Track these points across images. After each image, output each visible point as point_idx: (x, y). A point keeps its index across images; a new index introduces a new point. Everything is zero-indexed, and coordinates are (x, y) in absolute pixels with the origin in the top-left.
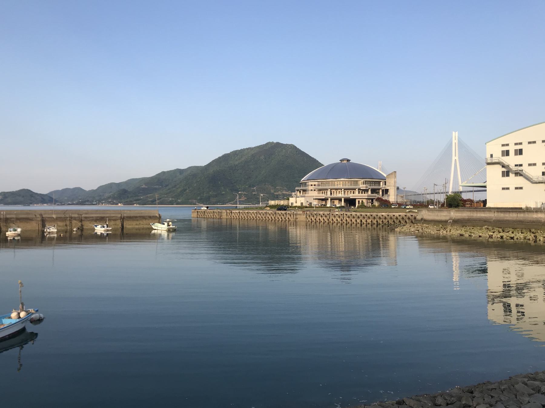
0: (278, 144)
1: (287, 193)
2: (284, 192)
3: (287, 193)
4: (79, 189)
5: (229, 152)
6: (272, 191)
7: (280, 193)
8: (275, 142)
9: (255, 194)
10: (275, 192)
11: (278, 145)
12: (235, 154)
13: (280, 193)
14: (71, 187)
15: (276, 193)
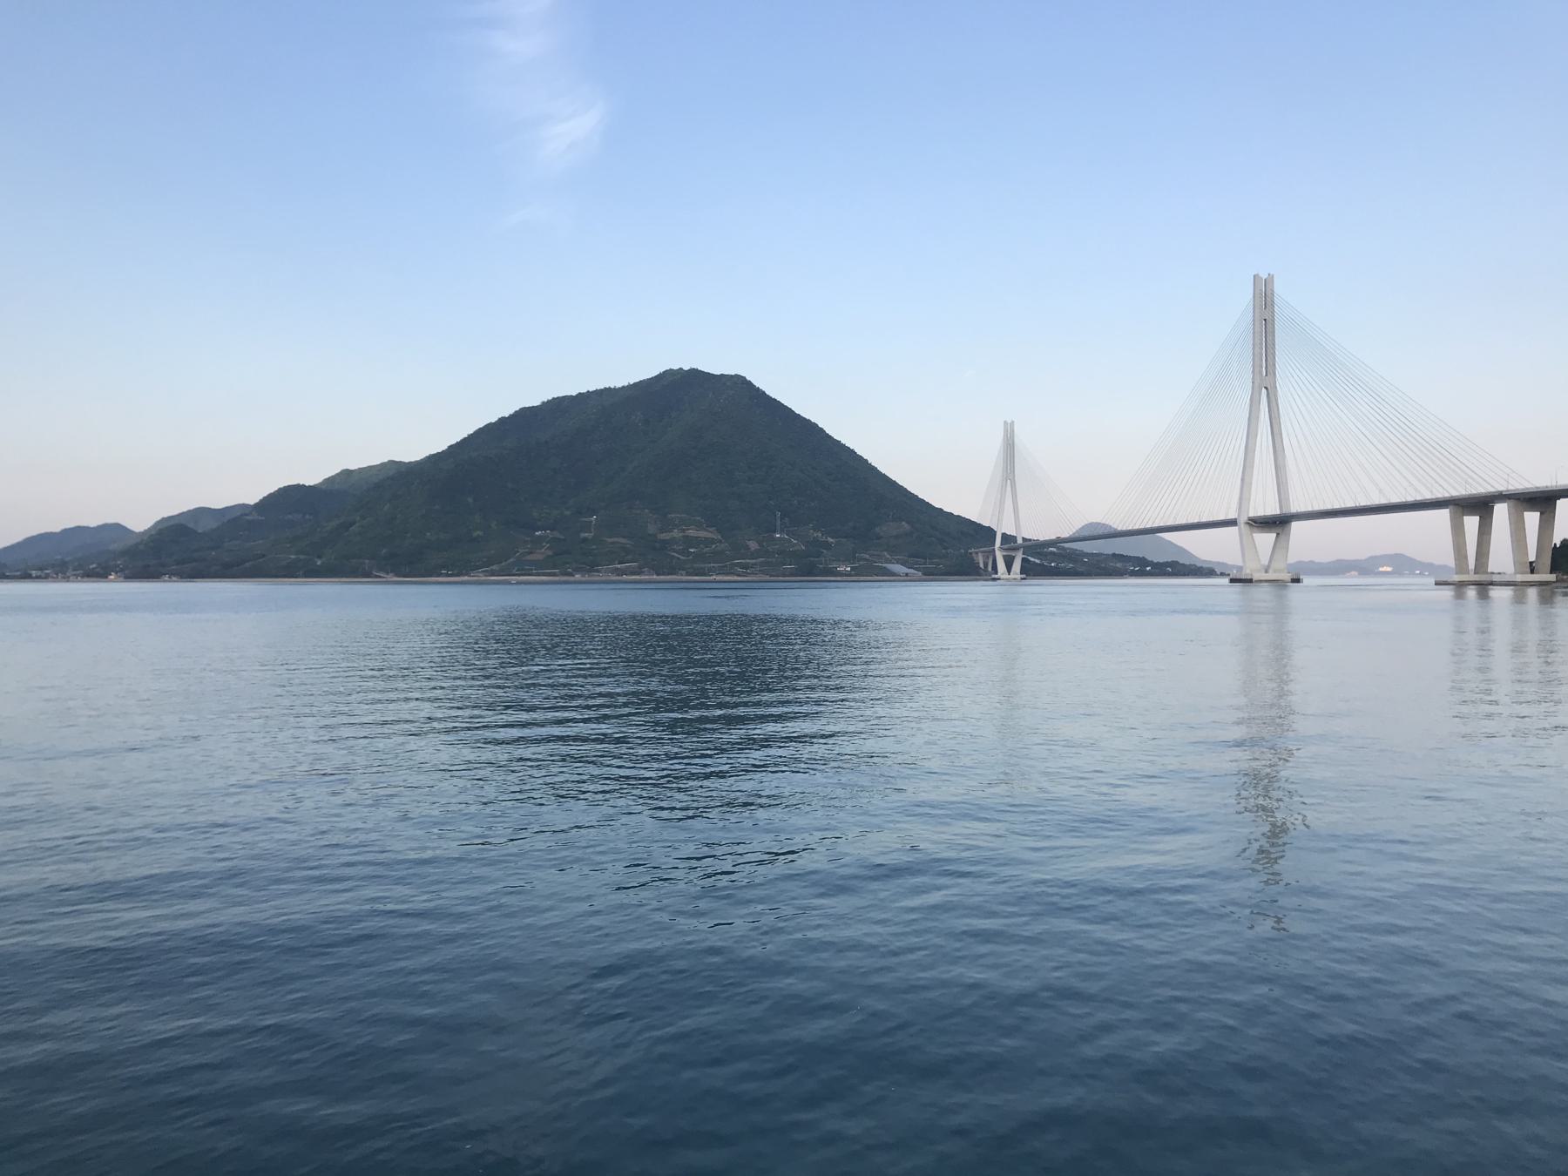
0: (695, 373)
1: (702, 534)
2: (691, 533)
3: (702, 534)
4: (117, 527)
5: (537, 403)
6: (651, 529)
7: (676, 534)
8: (686, 368)
9: (585, 540)
10: (662, 531)
11: (694, 378)
12: (558, 407)
13: (676, 534)
14: (93, 524)
15: (663, 536)
